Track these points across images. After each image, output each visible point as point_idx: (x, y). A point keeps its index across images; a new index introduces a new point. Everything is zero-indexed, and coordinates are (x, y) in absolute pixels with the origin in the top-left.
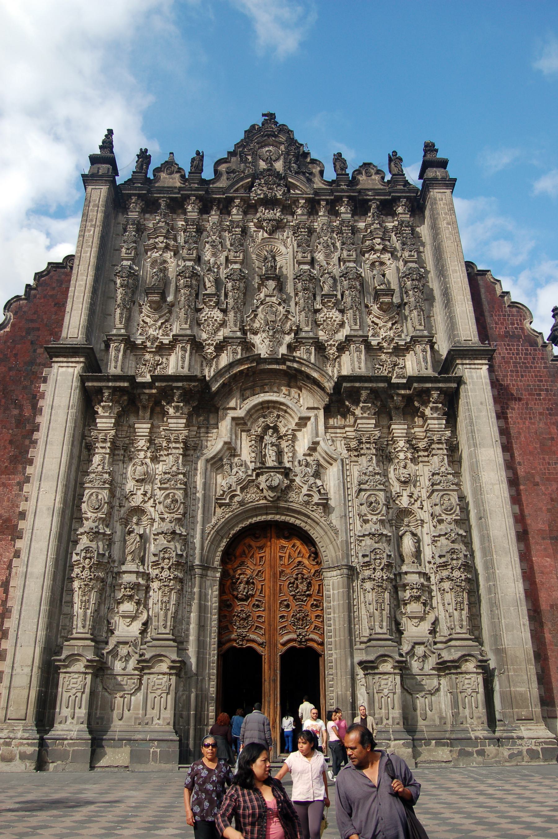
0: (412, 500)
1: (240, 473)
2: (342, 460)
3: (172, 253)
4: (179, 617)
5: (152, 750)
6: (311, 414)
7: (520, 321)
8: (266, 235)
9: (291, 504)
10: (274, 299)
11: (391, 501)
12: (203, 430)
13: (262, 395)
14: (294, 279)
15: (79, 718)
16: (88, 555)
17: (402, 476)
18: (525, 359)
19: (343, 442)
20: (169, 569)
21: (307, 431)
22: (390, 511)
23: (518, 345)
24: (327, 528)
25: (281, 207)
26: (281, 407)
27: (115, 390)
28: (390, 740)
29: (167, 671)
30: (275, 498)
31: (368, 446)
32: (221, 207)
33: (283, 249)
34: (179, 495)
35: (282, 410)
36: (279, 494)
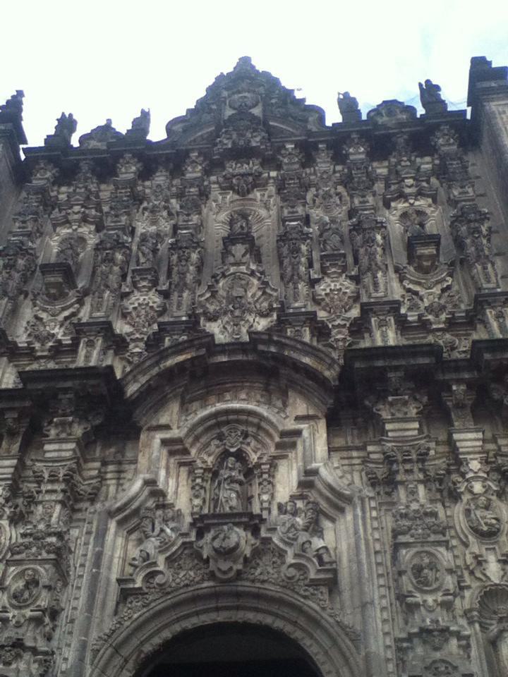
1: (168, 531)
2: (362, 500)
3: (93, 228)
6: (302, 426)
8: (236, 197)
9: (266, 586)
10: (243, 268)
12: (111, 468)
13: (217, 405)
14: (277, 241)
17: (482, 522)
19: (363, 473)
21: (296, 458)
22: (467, 594)
24: (335, 630)
25: (260, 160)
26: (250, 419)
30: (232, 574)
31: (408, 467)
32: (171, 165)
33: (263, 212)
35: (252, 424)
36: (240, 567)
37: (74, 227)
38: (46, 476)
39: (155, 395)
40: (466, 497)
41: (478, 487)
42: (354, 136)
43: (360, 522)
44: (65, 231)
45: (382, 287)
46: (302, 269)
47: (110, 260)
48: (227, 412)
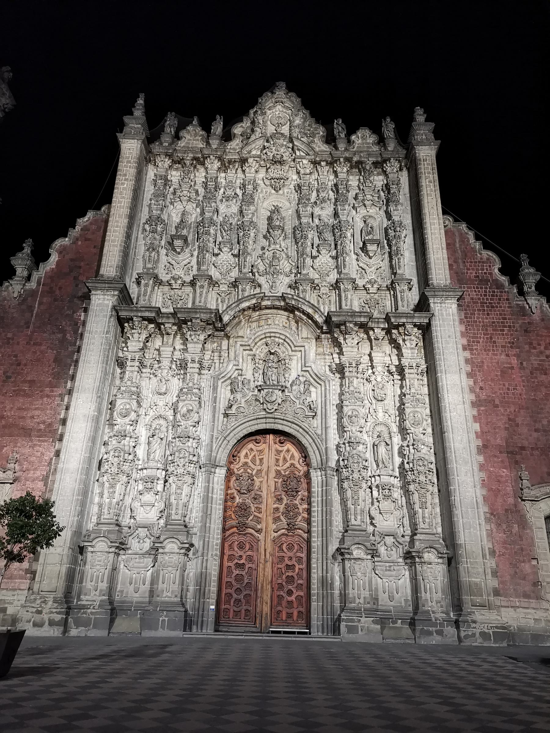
4: (190, 507)
5: (161, 619)
7: (490, 266)
8: (273, 191)
11: (369, 415)
15: (101, 591)
16: (116, 454)
18: (491, 299)
22: (369, 424)
23: (486, 288)
28: (361, 617)
29: (178, 551)
31: (351, 369)
36: (275, 408)
37: (184, 205)
38: (190, 360)
40: (374, 382)
42: (342, 160)
43: (328, 392)
44: (179, 207)
45: (347, 266)
47: (208, 233)
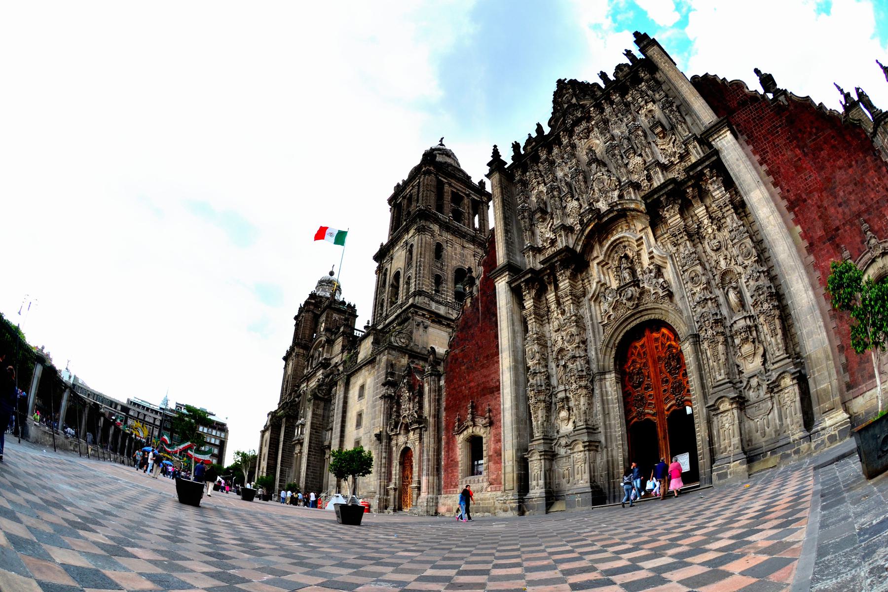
0: (728, 260)
6: (642, 234)
8: (586, 140)
11: (714, 270)
12: (586, 281)
20: (575, 382)
27: (527, 282)
31: (681, 236)
34: (574, 330)
36: (636, 302)
39: (588, 247)
40: (707, 237)
41: (710, 231)
46: (620, 161)
48: (615, 241)
